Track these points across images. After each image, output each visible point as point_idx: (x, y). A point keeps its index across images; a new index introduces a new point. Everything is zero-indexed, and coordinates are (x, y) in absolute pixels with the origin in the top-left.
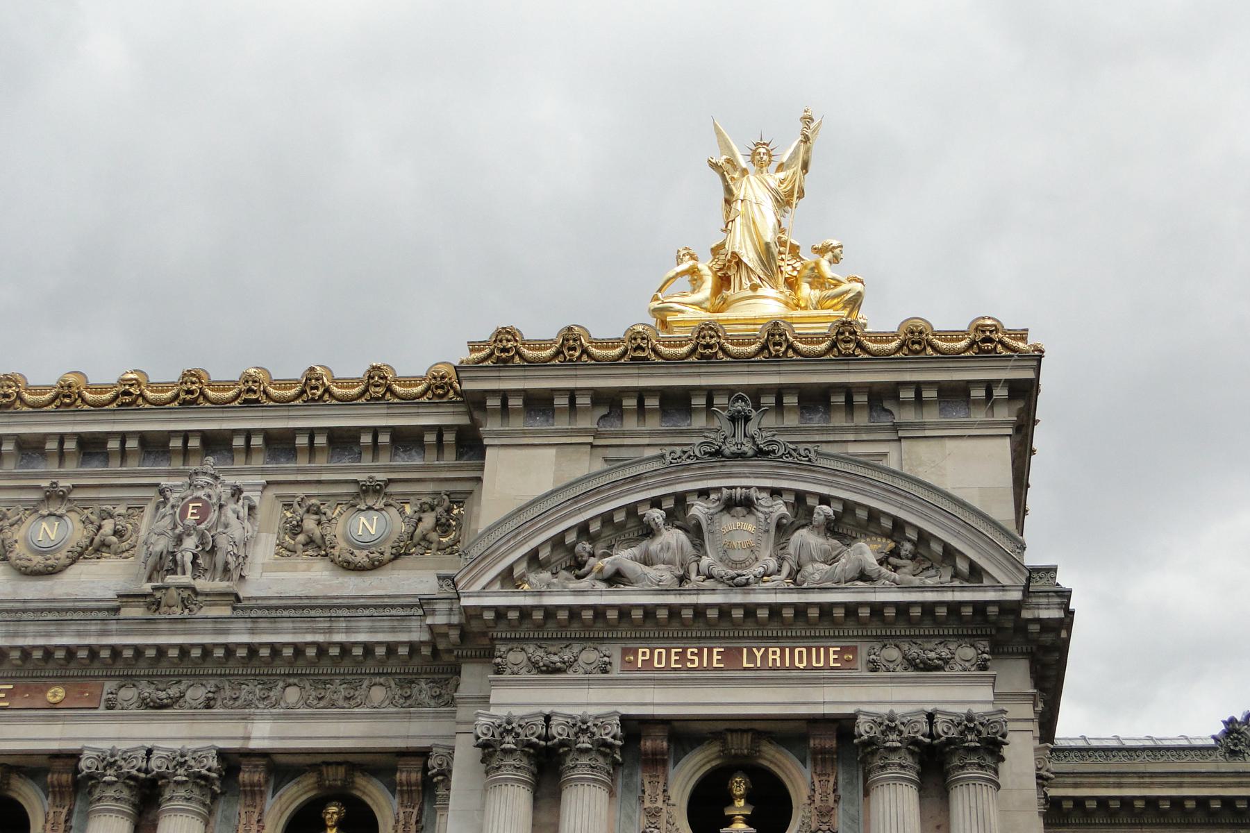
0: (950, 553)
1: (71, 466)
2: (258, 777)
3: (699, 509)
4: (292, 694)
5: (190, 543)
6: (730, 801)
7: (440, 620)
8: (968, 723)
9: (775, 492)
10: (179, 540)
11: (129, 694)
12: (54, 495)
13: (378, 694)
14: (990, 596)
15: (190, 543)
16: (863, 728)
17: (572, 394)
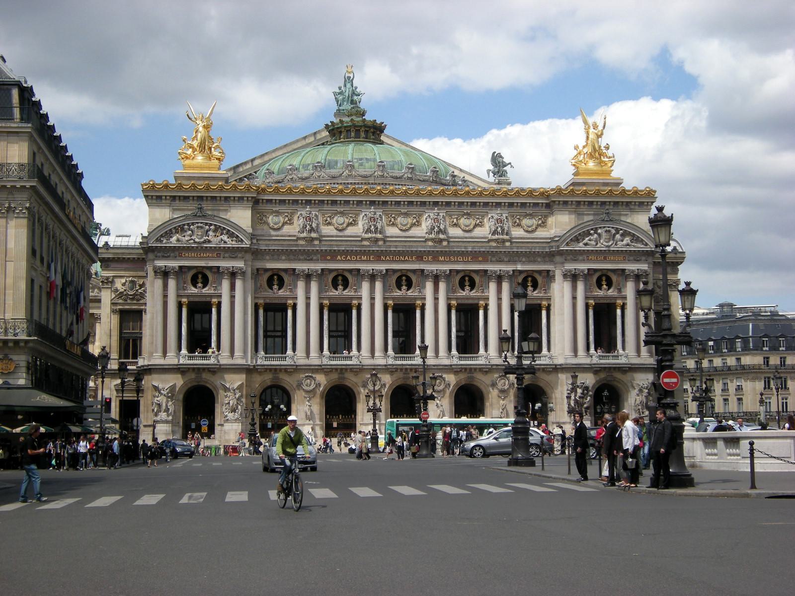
0: (642, 240)
1: (469, 208)
2: (518, 274)
3: (599, 231)
4: (524, 259)
5: (499, 229)
6: (602, 280)
8: (646, 271)
9: (613, 228)
10: (497, 228)
11: (494, 259)
12: (468, 214)
13: (539, 260)
15: (499, 229)
16: (627, 271)
17: (572, 201)
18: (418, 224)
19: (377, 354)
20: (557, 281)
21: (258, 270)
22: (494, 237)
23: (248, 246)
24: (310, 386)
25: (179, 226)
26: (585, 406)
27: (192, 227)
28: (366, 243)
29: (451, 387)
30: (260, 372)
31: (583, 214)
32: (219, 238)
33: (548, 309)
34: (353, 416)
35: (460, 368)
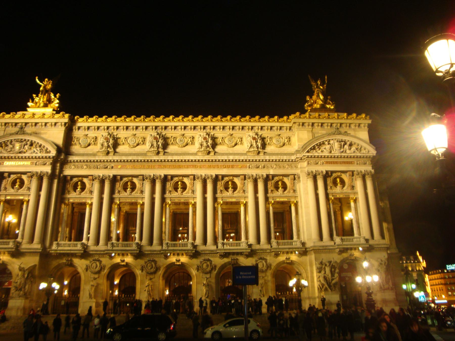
3: (331, 142)
5: (255, 143)
7: (298, 157)
14: (372, 155)
18: (193, 143)
19: (155, 241)
20: (301, 182)
21: (65, 177)
22: (250, 150)
23: (54, 155)
24: (96, 268)
25: (4, 142)
26: (334, 282)
27: (13, 142)
28: (149, 154)
29: (217, 269)
30: (54, 255)
31: (318, 133)
32: (32, 151)
33: (296, 205)
34: (134, 295)
35: (224, 252)
